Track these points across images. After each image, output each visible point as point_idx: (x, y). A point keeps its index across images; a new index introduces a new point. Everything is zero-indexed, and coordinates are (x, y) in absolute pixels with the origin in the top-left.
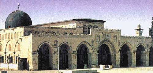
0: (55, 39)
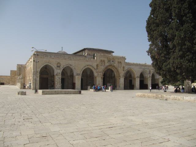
0: (58, 61)
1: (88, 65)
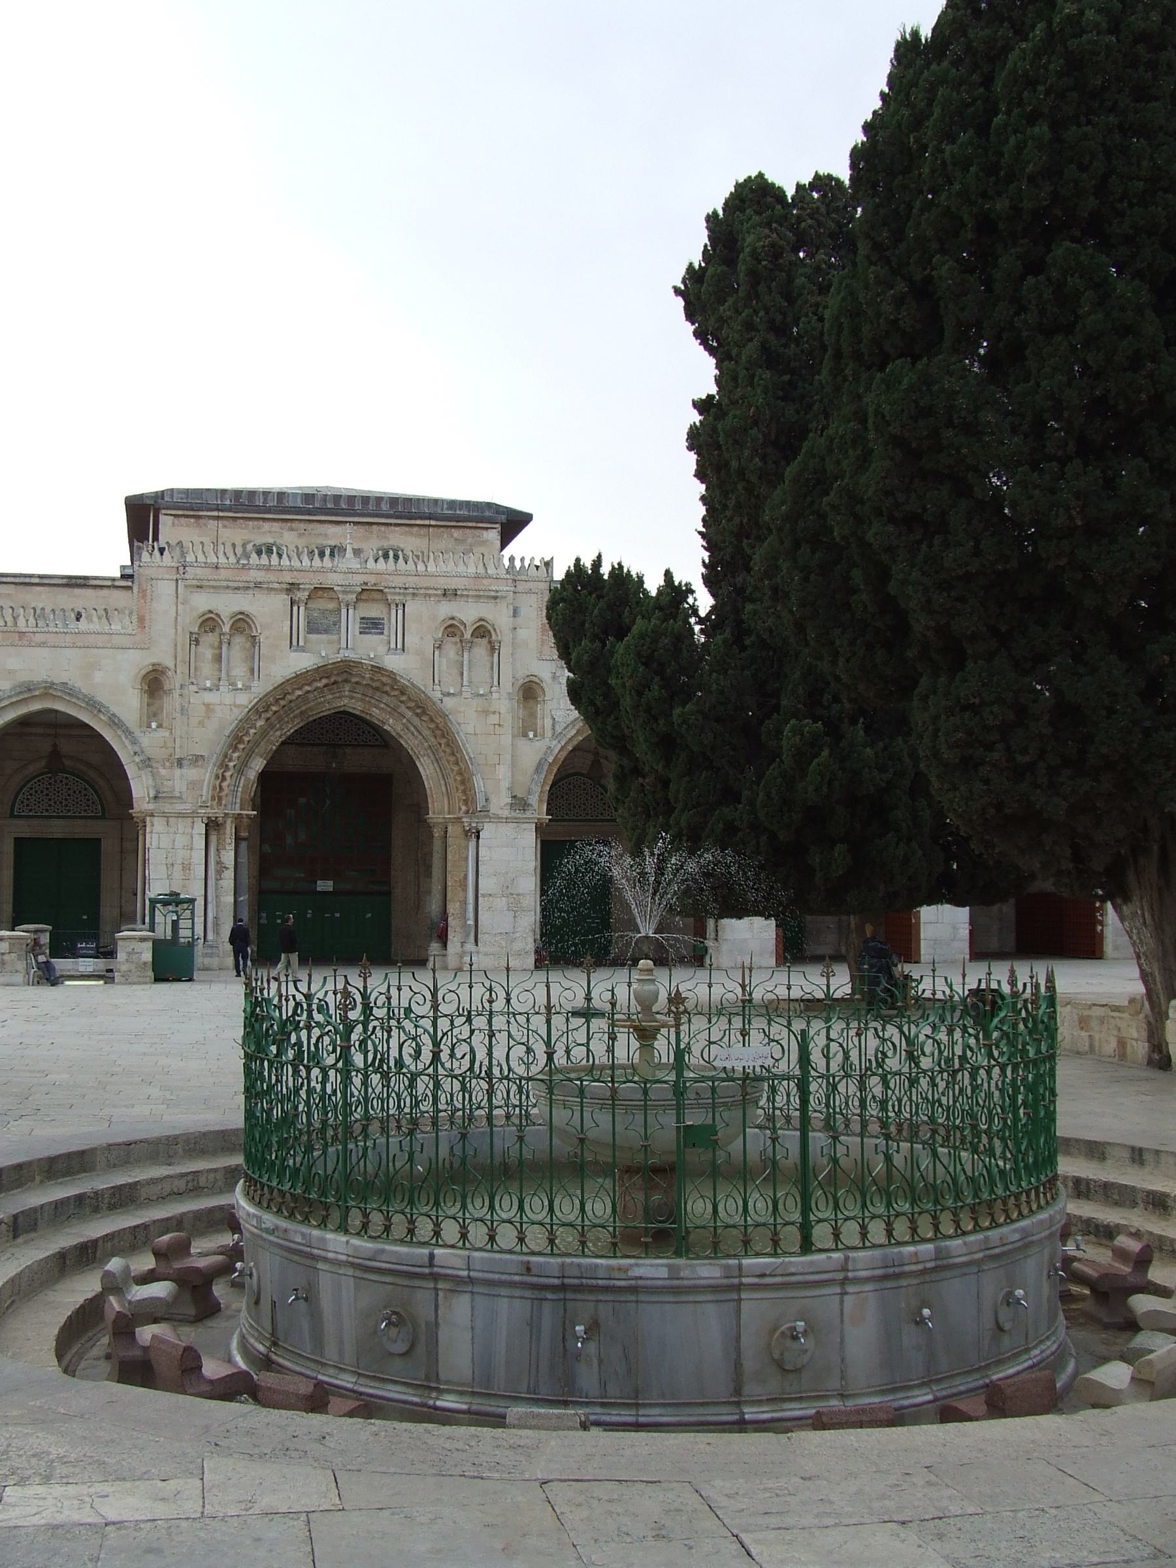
1: (24, 677)
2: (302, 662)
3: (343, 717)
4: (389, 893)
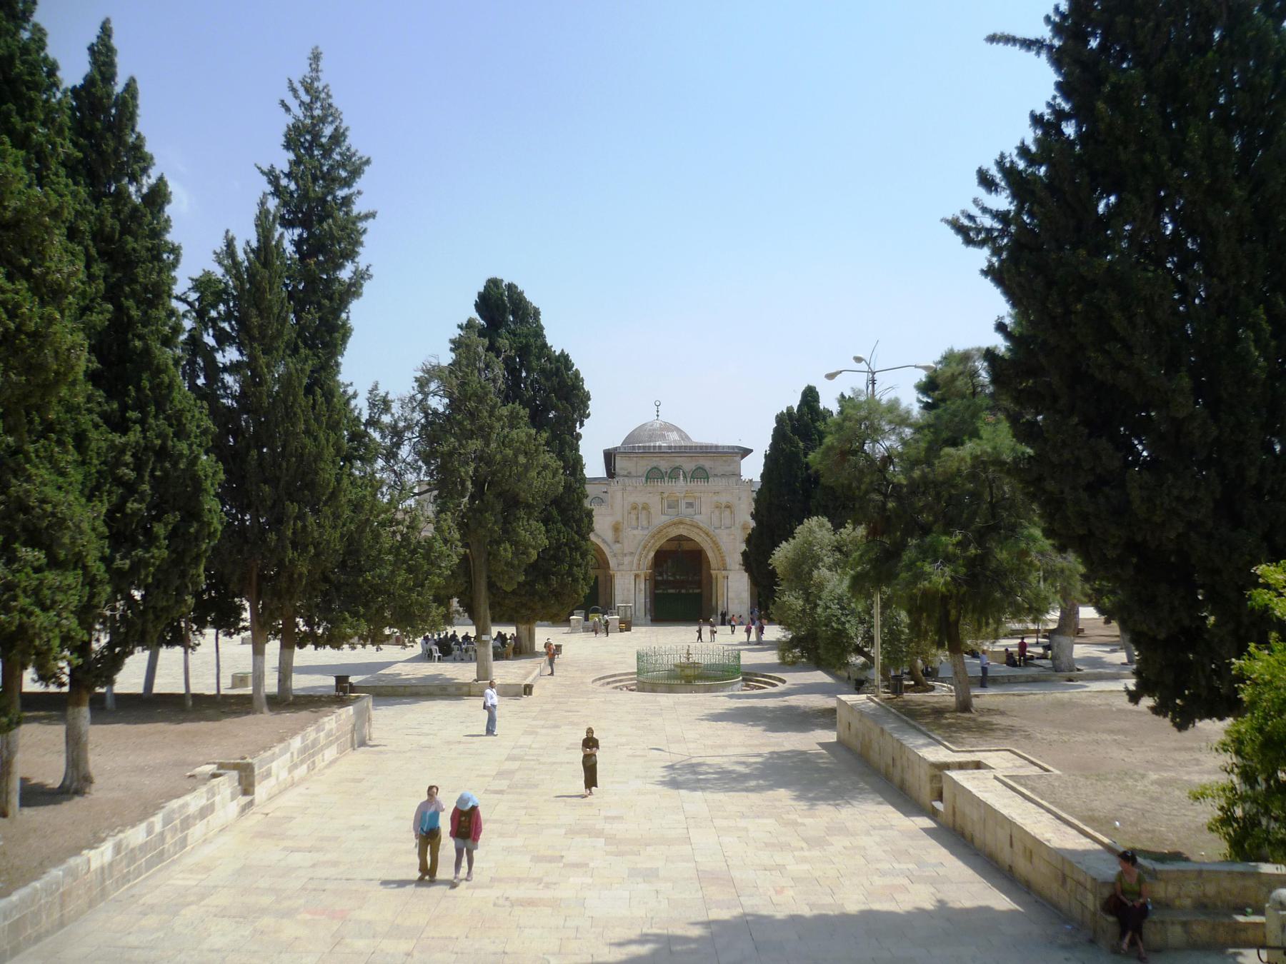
2: (664, 518)
3: (681, 536)
4: (700, 595)
